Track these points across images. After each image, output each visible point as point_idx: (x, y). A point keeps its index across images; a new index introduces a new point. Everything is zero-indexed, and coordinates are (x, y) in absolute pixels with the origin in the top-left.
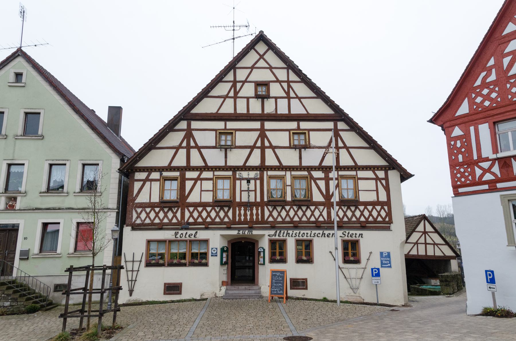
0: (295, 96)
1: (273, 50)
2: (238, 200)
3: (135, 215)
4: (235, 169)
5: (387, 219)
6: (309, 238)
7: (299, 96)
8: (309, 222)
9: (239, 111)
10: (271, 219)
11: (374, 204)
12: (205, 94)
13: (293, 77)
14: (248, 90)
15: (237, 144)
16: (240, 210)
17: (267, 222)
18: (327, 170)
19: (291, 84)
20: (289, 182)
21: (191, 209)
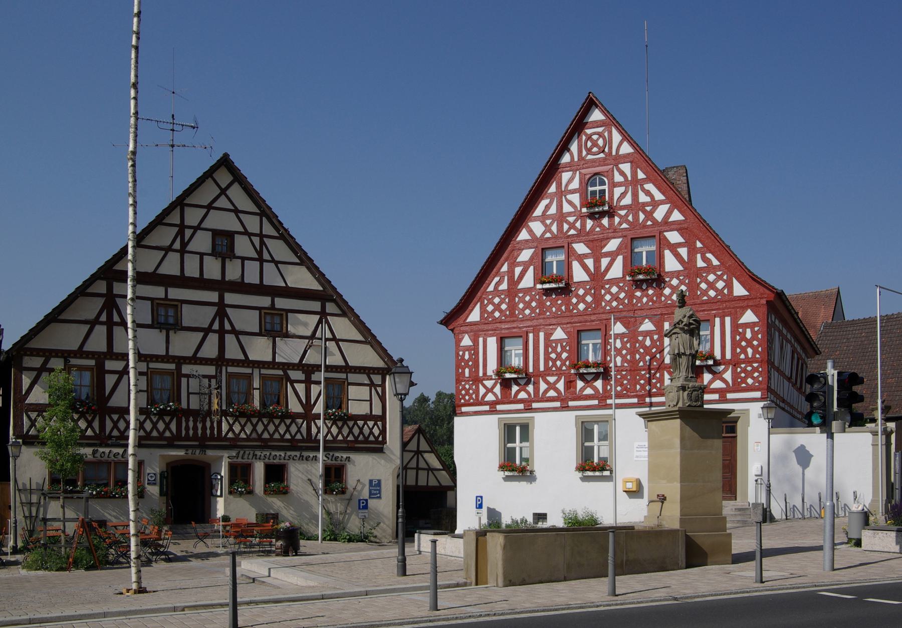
0: (270, 259)
1: (241, 184)
2: (184, 405)
4: (180, 361)
5: (380, 439)
6: (282, 461)
7: (276, 259)
8: (282, 438)
9: (188, 273)
10: (230, 435)
11: (366, 418)
13: (268, 229)
14: (202, 242)
15: (185, 324)
16: (187, 421)
17: (226, 439)
18: (310, 370)
19: (265, 239)
20: (256, 384)
21: (115, 417)
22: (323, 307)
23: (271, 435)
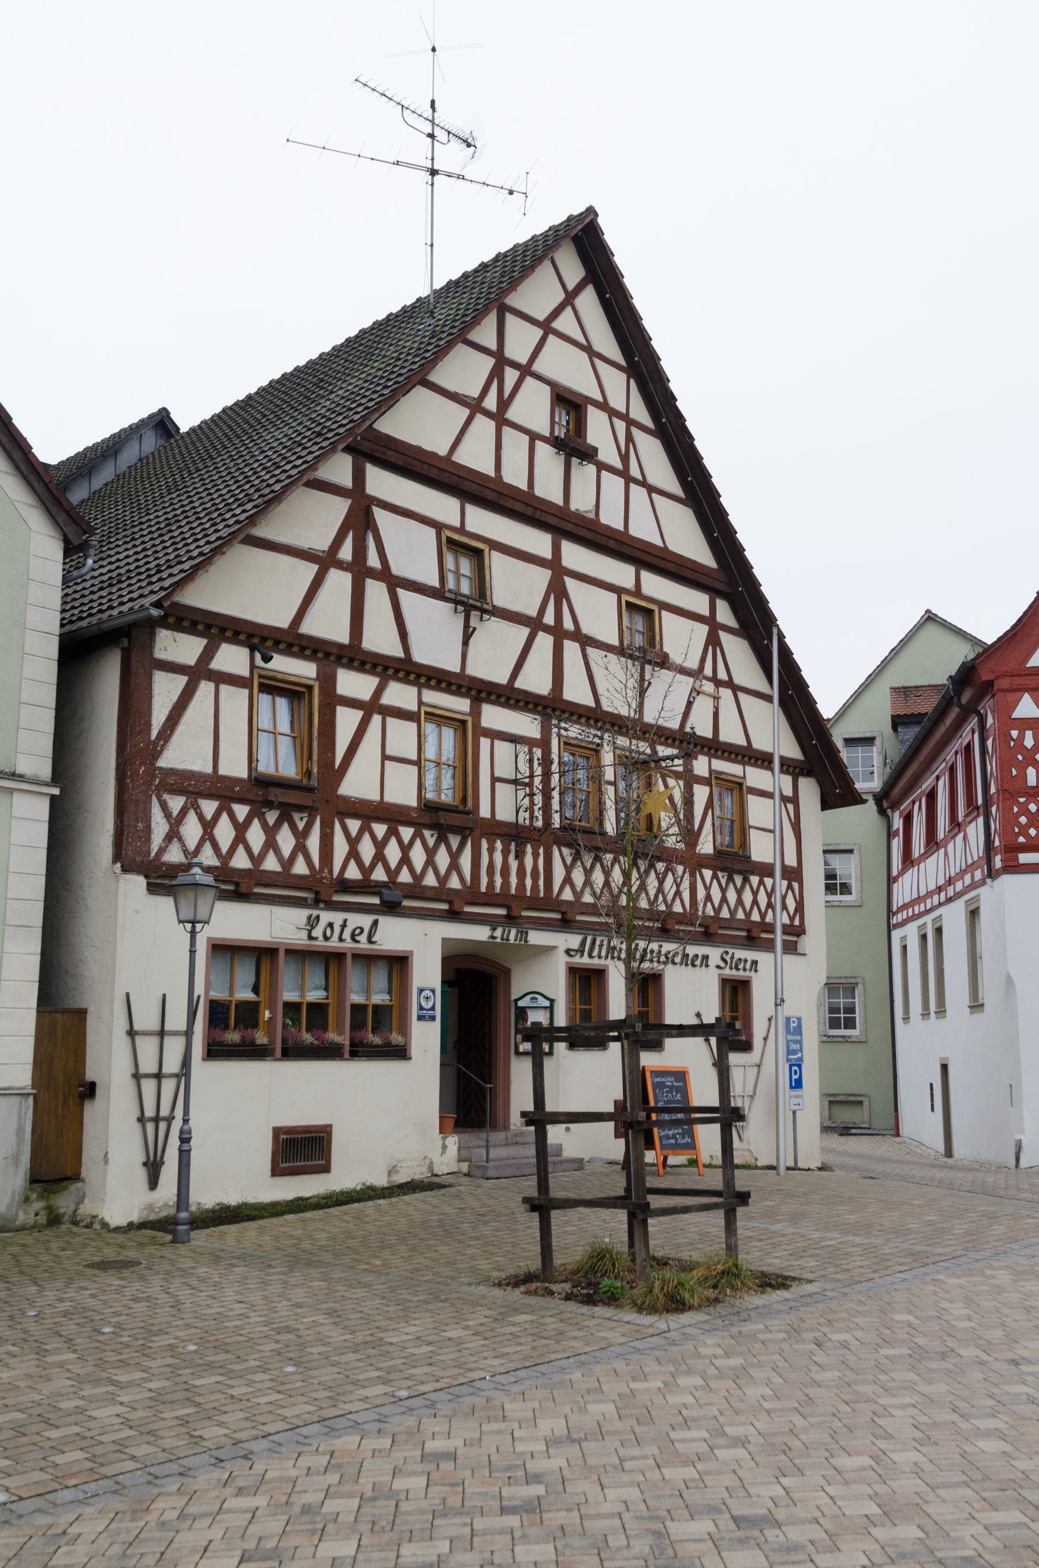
2: (485, 812)
3: (160, 827)
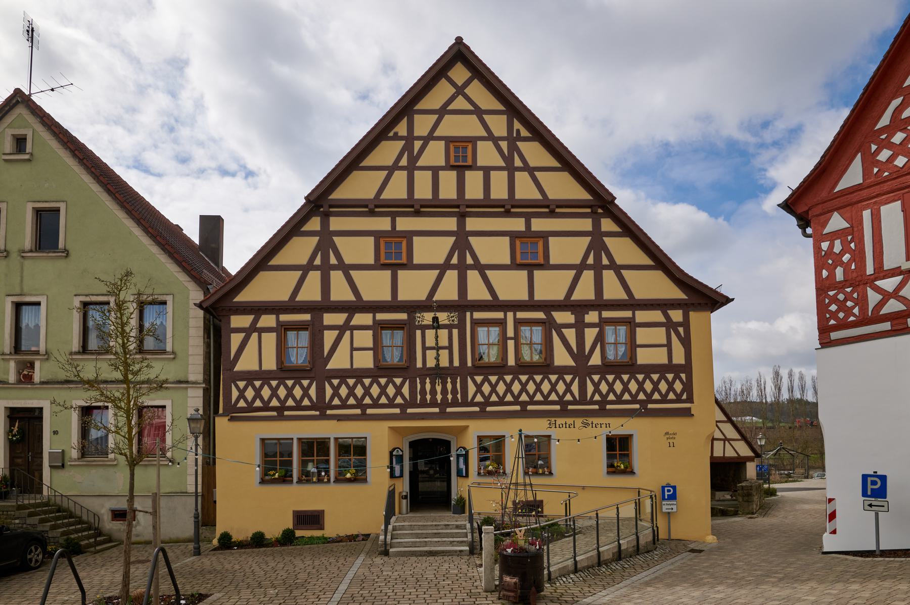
3: (235, 394)
4: (413, 308)
5: (684, 397)
11: (661, 369)
12: (353, 162)
14: (435, 154)
18: (579, 308)
20: (510, 333)
22: (597, 225)
23: (531, 397)
